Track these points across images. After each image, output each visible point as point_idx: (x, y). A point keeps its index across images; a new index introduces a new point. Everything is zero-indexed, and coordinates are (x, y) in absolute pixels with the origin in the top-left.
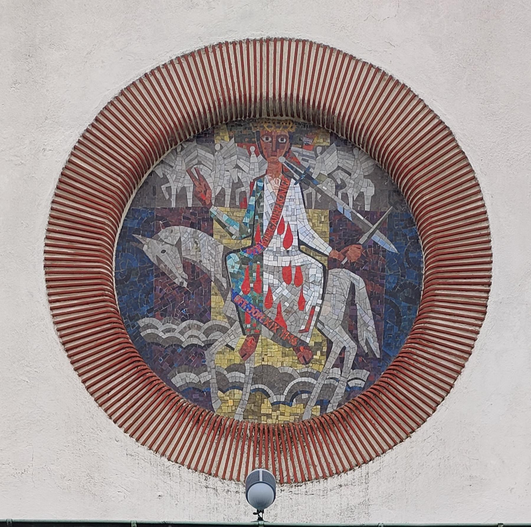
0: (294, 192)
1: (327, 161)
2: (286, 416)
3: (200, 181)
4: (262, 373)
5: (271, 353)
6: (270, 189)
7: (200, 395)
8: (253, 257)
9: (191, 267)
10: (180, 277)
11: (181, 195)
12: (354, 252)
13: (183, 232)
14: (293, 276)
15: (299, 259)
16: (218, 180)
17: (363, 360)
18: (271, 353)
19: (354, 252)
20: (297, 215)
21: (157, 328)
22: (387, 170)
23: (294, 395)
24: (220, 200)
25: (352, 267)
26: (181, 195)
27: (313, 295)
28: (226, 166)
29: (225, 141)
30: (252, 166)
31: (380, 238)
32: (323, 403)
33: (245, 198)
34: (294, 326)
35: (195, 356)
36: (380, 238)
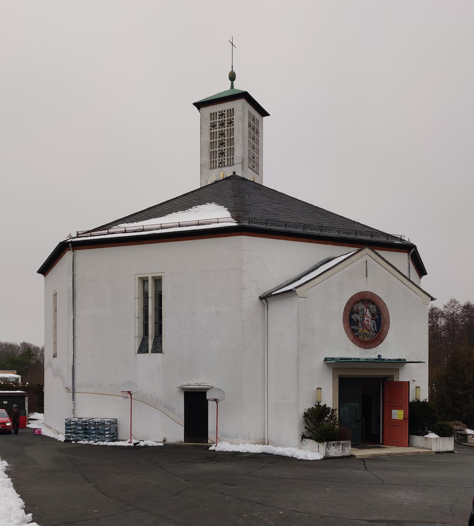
0: (368, 310)
1: (371, 306)
3: (358, 308)
4: (364, 333)
5: (366, 331)
6: (365, 309)
8: (363, 319)
9: (357, 319)
12: (374, 318)
13: (356, 315)
14: (368, 321)
15: (368, 319)
17: (375, 332)
18: (366, 331)
19: (374, 318)
20: (368, 313)
21: (353, 327)
22: (377, 308)
27: (370, 323)
28: (361, 306)
29: (360, 303)
30: (363, 306)
35: (357, 331)
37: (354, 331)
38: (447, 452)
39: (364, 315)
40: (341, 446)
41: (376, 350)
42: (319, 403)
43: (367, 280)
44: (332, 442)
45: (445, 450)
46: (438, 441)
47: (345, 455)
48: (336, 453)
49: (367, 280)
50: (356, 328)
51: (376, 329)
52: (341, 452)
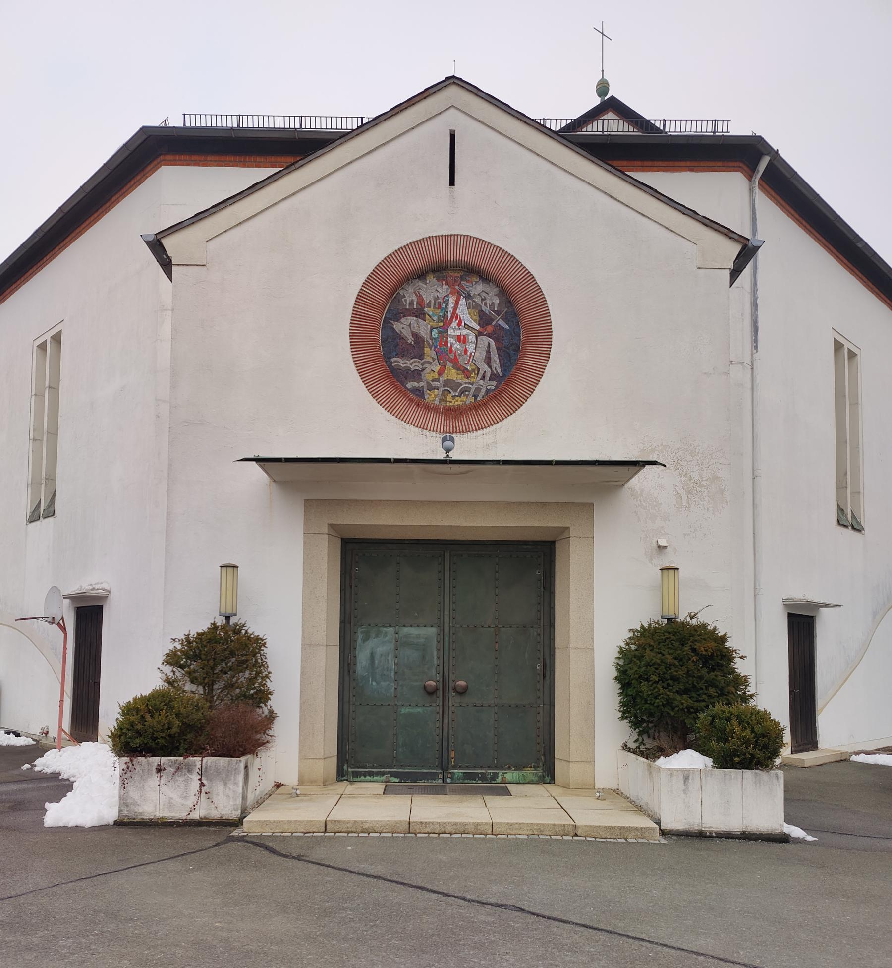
0: (463, 301)
1: (478, 288)
2: (458, 402)
3: (420, 297)
4: (447, 383)
5: (452, 374)
7: (419, 392)
9: (416, 336)
10: (411, 340)
11: (411, 303)
12: (490, 329)
13: (412, 320)
14: (462, 339)
15: (465, 332)
16: (428, 297)
18: (452, 374)
19: (490, 329)
21: (400, 362)
22: (504, 293)
23: (462, 392)
24: (429, 305)
25: (489, 336)
26: (411, 303)
27: (471, 348)
28: (432, 290)
29: (431, 279)
30: (444, 290)
31: (501, 323)
32: (475, 396)
33: (441, 304)
34: (461, 362)
35: (417, 375)
36: (501, 323)
37: (398, 377)
38: (747, 837)
40: (195, 777)
42: (228, 618)
43: (452, 197)
44: (156, 760)
45: (735, 825)
46: (694, 784)
47: (215, 814)
48: (170, 805)
49: (452, 197)
50: (413, 365)
52: (193, 799)
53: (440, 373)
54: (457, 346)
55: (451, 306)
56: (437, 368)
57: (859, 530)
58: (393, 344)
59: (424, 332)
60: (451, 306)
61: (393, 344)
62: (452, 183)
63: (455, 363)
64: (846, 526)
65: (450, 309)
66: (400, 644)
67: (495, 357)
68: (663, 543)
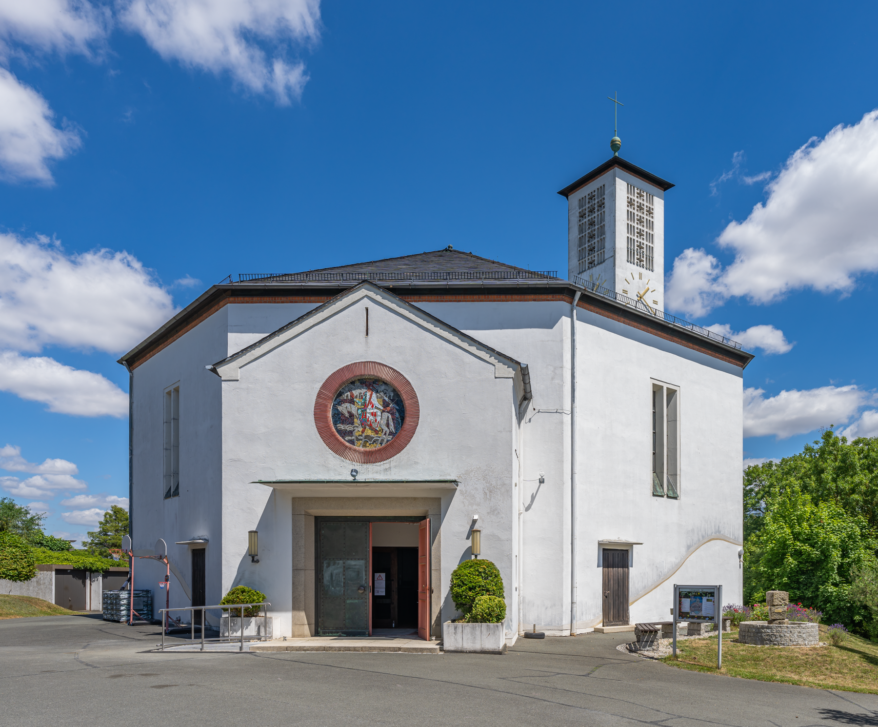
0: (374, 395)
4: (366, 437)
5: (369, 432)
6: (368, 394)
8: (364, 411)
9: (349, 412)
10: (347, 415)
13: (347, 405)
15: (375, 410)
18: (369, 432)
19: (388, 409)
20: (375, 400)
21: (342, 427)
32: (381, 444)
35: (351, 433)
39: (365, 406)
41: (387, 466)
43: (367, 342)
49: (367, 342)
50: (349, 428)
51: (392, 427)
53: (363, 432)
54: (371, 418)
55: (368, 397)
56: (361, 429)
57: (675, 498)
58: (338, 417)
59: (354, 412)
60: (368, 397)
61: (338, 417)
62: (367, 334)
63: (370, 426)
64: (662, 496)
65: (368, 399)
66: (346, 569)
67: (391, 423)
68: (476, 517)
